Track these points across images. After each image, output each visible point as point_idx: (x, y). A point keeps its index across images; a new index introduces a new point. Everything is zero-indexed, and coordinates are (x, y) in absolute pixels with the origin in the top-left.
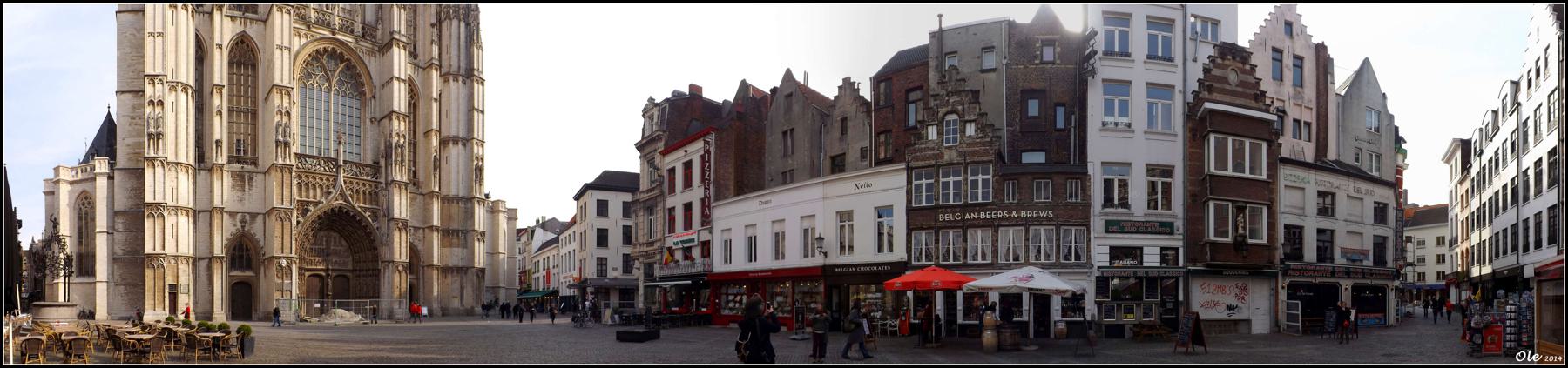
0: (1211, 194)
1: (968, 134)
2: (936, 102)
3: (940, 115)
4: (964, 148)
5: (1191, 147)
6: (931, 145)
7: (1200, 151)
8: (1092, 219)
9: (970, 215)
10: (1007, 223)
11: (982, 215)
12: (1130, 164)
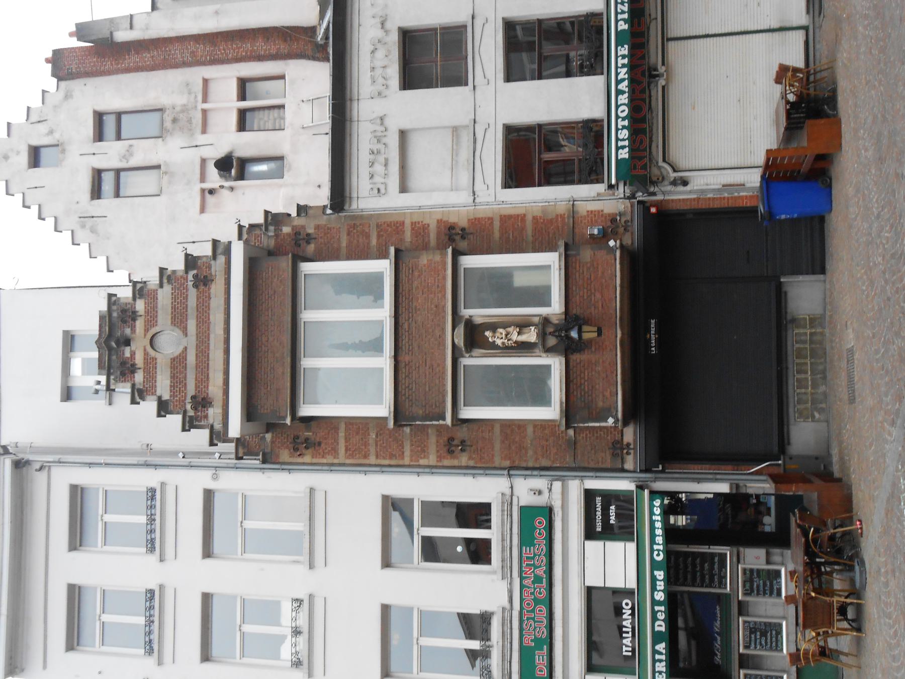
0: (444, 419)
5: (334, 452)
7: (342, 426)
12: (386, 610)
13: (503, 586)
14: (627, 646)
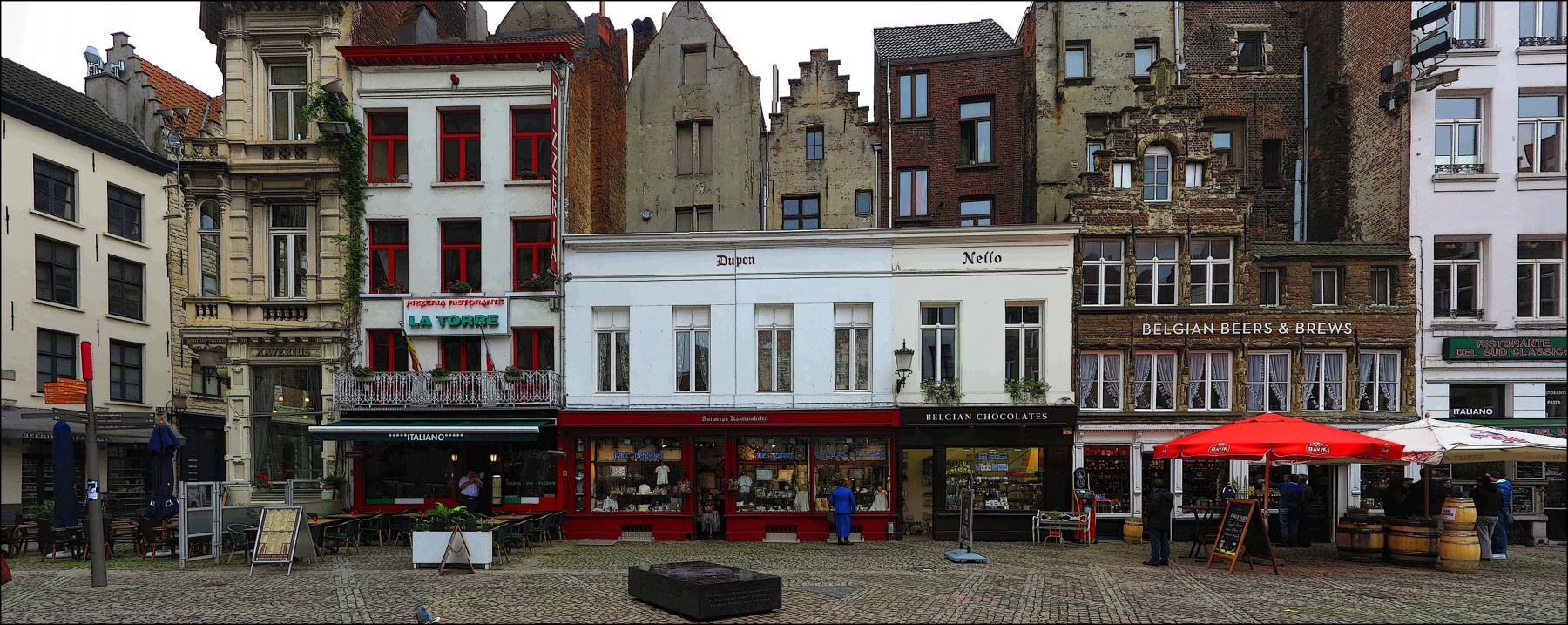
1: (1189, 182)
2: (1132, 121)
3: (1141, 145)
4: (1186, 208)
6: (1123, 198)
8: (1418, 337)
9: (1201, 327)
10: (1266, 344)
11: (1224, 328)
13: (1511, 324)
14: (1460, 412)
